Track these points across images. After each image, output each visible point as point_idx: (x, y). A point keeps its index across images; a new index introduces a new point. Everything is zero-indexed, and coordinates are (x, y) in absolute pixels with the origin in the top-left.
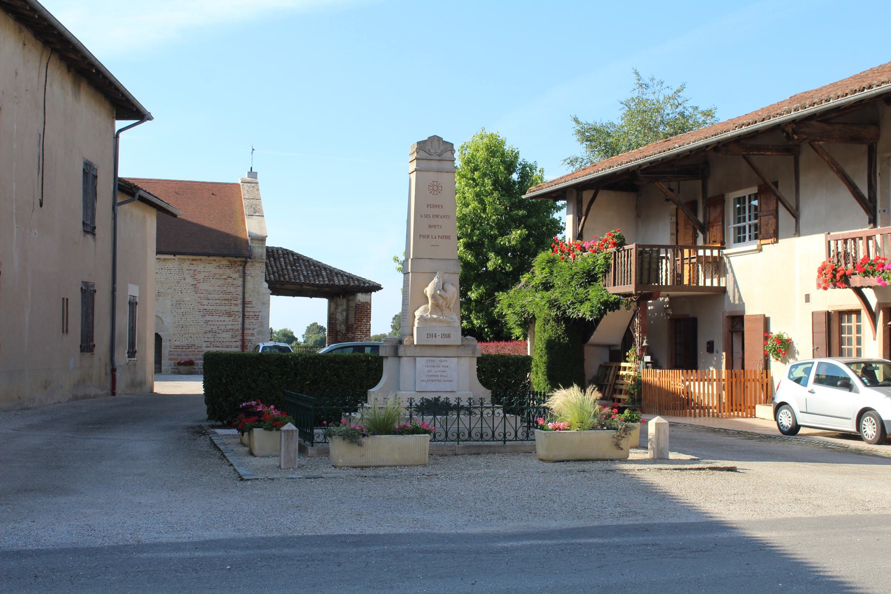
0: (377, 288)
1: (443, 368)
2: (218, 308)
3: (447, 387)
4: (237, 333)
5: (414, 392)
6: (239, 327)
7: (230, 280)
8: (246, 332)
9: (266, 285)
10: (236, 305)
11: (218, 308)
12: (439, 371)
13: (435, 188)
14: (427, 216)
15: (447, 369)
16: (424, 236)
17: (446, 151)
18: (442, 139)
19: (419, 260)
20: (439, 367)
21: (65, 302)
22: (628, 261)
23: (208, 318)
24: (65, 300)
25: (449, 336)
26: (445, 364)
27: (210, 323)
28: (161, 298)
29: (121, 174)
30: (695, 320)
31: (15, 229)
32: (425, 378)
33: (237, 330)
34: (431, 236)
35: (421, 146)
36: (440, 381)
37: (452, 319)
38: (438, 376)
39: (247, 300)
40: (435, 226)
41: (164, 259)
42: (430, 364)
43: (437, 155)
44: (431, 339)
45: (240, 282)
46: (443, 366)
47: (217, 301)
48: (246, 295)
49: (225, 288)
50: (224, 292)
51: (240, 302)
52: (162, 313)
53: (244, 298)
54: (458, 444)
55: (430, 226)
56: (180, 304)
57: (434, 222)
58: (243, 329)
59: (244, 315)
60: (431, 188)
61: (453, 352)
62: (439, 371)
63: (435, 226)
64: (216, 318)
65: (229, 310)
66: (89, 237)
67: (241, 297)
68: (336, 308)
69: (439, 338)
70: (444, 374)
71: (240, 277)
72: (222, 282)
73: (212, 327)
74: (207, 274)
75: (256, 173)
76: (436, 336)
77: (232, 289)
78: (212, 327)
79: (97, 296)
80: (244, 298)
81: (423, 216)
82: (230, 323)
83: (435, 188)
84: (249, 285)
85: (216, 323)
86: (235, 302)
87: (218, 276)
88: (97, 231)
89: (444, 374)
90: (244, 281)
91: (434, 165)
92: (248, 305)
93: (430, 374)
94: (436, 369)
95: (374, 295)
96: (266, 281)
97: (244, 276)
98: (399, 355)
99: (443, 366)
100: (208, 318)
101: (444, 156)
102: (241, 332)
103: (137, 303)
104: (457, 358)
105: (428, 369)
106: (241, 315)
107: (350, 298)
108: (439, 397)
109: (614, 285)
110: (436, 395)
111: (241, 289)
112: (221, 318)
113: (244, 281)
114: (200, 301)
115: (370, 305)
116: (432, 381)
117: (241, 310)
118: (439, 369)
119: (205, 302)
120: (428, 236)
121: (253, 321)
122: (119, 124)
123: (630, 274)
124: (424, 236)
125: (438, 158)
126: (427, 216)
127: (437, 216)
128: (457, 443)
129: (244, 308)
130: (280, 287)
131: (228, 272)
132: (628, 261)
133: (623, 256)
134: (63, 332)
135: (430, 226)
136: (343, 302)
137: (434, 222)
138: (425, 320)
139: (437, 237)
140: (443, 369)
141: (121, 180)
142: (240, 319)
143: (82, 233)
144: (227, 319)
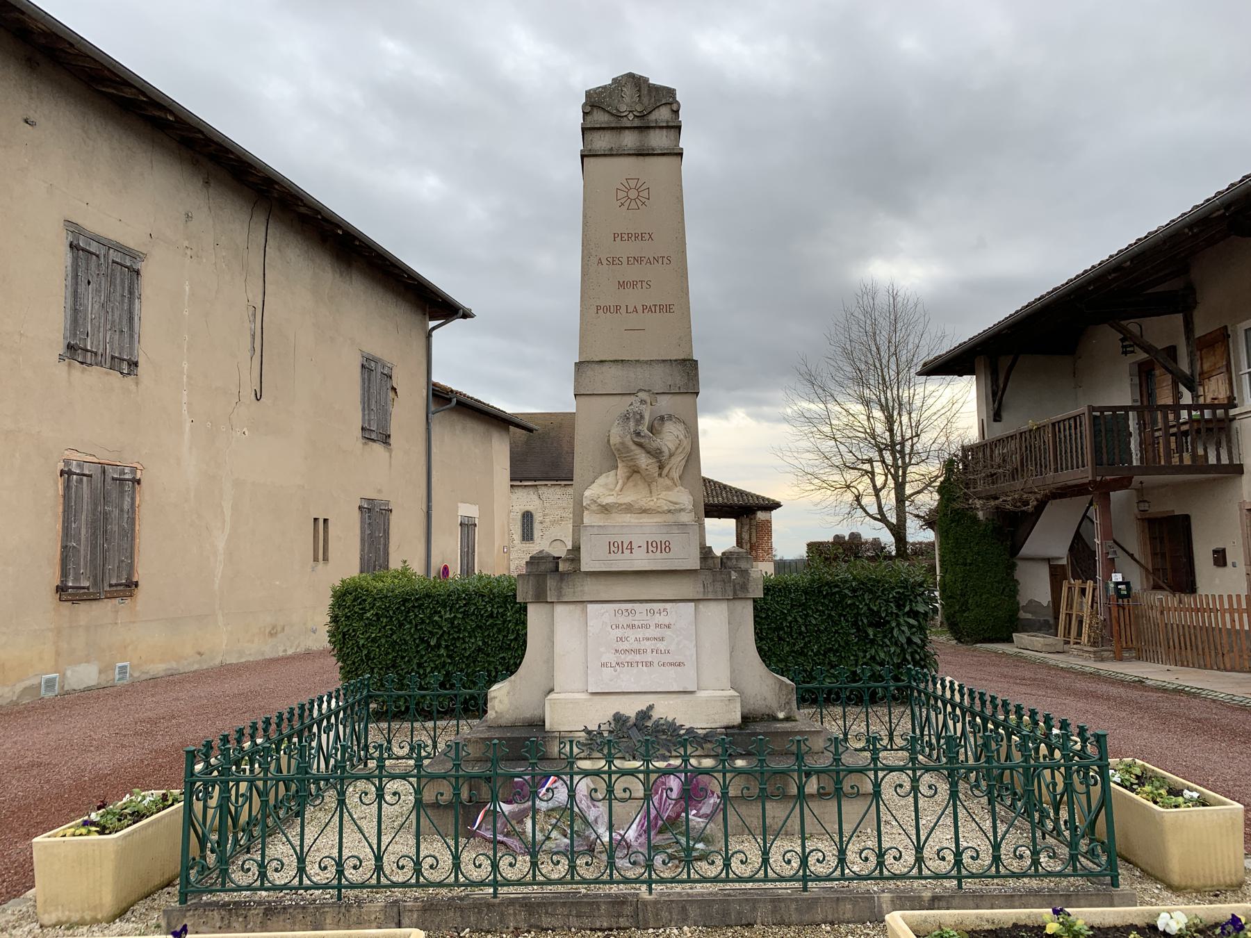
0: (777, 505)
3: (670, 679)
5: (584, 696)
12: (648, 639)
13: (633, 194)
14: (613, 261)
15: (668, 632)
16: (607, 309)
18: (646, 80)
19: (596, 366)
20: (647, 627)
21: (321, 526)
22: (1076, 434)
24: (321, 522)
25: (665, 547)
29: (435, 379)
30: (1186, 519)
31: (188, 425)
32: (610, 657)
34: (623, 310)
35: (595, 102)
36: (651, 663)
38: (645, 651)
40: (634, 284)
42: (622, 620)
43: (635, 116)
44: (619, 555)
46: (657, 626)
55: (622, 285)
61: (687, 588)
62: (648, 639)
63: (634, 284)
66: (378, 448)
68: (742, 528)
70: (661, 646)
76: (631, 549)
79: (394, 518)
81: (605, 262)
83: (633, 194)
88: (392, 441)
89: (661, 646)
91: (629, 140)
93: (626, 646)
94: (640, 634)
95: (774, 512)
98: (549, 600)
99: (657, 626)
101: (653, 117)
103: (475, 525)
104: (693, 604)
105: (619, 633)
107: (752, 517)
108: (651, 707)
109: (1056, 470)
110: (638, 705)
115: (770, 522)
116: (631, 664)
120: (618, 309)
122: (432, 324)
123: (1082, 453)
124: (607, 309)
125: (637, 123)
126: (613, 261)
127: (639, 260)
128: (644, 887)
132: (1076, 434)
133: (1067, 427)
134: (316, 559)
135: (622, 285)
136: (745, 520)
138: (603, 506)
139: (640, 309)
140: (657, 633)
141: (435, 385)
143: (361, 441)
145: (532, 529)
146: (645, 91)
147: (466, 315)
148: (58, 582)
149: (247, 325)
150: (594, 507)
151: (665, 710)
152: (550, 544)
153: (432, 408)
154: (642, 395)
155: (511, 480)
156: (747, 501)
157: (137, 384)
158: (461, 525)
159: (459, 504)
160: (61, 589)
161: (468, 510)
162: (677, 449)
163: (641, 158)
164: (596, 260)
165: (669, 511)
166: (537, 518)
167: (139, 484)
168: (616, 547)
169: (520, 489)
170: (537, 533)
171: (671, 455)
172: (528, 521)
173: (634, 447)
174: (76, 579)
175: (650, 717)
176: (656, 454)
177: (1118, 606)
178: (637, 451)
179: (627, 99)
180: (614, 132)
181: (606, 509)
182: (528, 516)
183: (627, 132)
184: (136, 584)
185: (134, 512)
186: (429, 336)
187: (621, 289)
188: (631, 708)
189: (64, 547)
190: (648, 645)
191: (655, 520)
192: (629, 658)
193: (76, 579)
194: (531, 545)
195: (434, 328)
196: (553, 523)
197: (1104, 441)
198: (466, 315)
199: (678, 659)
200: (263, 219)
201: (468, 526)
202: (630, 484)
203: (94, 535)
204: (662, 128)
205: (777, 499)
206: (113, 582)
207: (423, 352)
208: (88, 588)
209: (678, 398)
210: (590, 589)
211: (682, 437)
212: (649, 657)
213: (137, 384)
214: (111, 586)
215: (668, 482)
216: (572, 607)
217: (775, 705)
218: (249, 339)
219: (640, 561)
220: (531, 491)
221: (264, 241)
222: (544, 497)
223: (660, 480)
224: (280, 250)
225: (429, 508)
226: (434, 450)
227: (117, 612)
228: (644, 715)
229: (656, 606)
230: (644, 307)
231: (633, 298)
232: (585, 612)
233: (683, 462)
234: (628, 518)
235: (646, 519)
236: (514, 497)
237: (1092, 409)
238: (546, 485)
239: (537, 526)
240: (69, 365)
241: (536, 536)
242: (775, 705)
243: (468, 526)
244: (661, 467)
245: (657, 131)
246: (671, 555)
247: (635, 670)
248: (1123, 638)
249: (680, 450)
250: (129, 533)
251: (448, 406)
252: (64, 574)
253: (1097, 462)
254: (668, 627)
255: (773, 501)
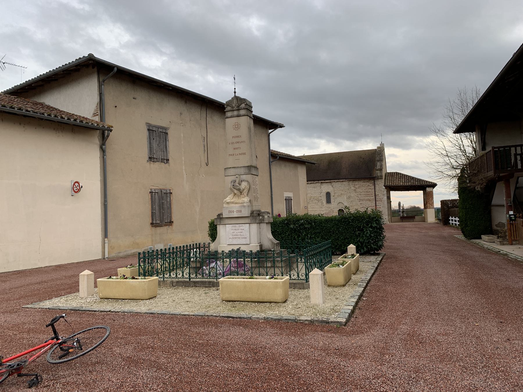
1: (241, 230)
2: (365, 198)
3: (244, 241)
4: (374, 207)
5: (226, 245)
6: (374, 205)
7: (369, 187)
8: (377, 207)
9: (384, 188)
10: (372, 196)
11: (365, 198)
12: (239, 232)
13: (237, 126)
14: (233, 143)
16: (231, 155)
17: (242, 104)
19: (229, 169)
20: (239, 230)
23: (361, 202)
25: (241, 211)
26: (243, 228)
27: (362, 204)
28: (342, 196)
31: (185, 176)
32: (231, 237)
33: (374, 206)
37: (244, 201)
39: (376, 194)
40: (237, 148)
41: (342, 181)
42: (234, 228)
45: (373, 187)
46: (241, 229)
47: (364, 196)
48: (376, 192)
49: (367, 190)
50: (367, 192)
51: (374, 195)
52: (343, 201)
53: (375, 193)
54: (217, 280)
55: (234, 149)
56: (350, 198)
57: (237, 146)
58: (376, 206)
59: (376, 200)
60: (234, 127)
61: (247, 221)
62: (239, 232)
63: (237, 148)
64: (365, 202)
65: (369, 198)
67: (374, 193)
69: (235, 213)
70: (242, 234)
71: (373, 185)
72: (366, 188)
73: (363, 206)
74: (360, 185)
75: (384, 144)
77: (370, 190)
78: (363, 206)
80: (375, 193)
82: (370, 204)
83: (237, 126)
84: (377, 188)
85: (365, 204)
86: (372, 195)
87: (364, 186)
89: (242, 234)
90: (375, 187)
91: (235, 113)
92: (377, 196)
93: (234, 234)
96: (384, 186)
97: (374, 185)
99: (241, 229)
100: (361, 202)
101: (241, 106)
102: (375, 207)
104: (248, 224)
105: (233, 231)
106: (374, 200)
108: (240, 248)
109: (487, 172)
110: (237, 247)
111: (373, 190)
112: (367, 202)
113: (375, 187)
114: (358, 196)
116: (235, 238)
117: (374, 198)
118: (239, 231)
119: (360, 196)
121: (380, 202)
122: (270, 131)
124: (231, 155)
126: (233, 143)
127: (238, 142)
129: (375, 197)
130: (390, 188)
131: (368, 184)
135: (234, 149)
137: (237, 146)
139: (238, 154)
140: (241, 231)
142: (374, 202)
144: (369, 202)
145: (330, 199)
146: (239, 100)
147: (285, 126)
148: (151, 222)
149: (202, 143)
150: (225, 203)
151: (243, 248)
152: (338, 204)
153: (271, 160)
154: (237, 176)
155: (307, 181)
156: (421, 183)
157: (169, 166)
158: (285, 199)
159: (284, 193)
160: (152, 224)
161: (290, 195)
162: (245, 188)
163: (238, 117)
164: (228, 143)
165: (242, 203)
166: (332, 194)
167: (172, 194)
168: (230, 212)
169: (325, 184)
170: (332, 200)
171: (244, 190)
172: (328, 196)
173: (233, 189)
174: (156, 221)
175: (239, 250)
176: (239, 190)
177: (510, 224)
178: (234, 189)
179: (235, 103)
180: (232, 111)
181: (228, 203)
182: (328, 194)
183: (235, 111)
184: (173, 222)
185: (171, 202)
186: (269, 136)
187: (234, 150)
188: (235, 248)
189: (152, 212)
190: (239, 234)
191: (239, 205)
192: (235, 237)
193: (156, 221)
194: (330, 205)
195: (270, 133)
196: (338, 196)
197: (500, 160)
198: (284, 127)
199: (245, 237)
200: (205, 109)
201: (288, 200)
202: (235, 197)
203: (160, 209)
204: (242, 109)
205: (435, 182)
206: (166, 221)
207: (267, 142)
208: (159, 223)
209: (247, 175)
210: (227, 221)
211: (246, 185)
212: (239, 237)
213: (169, 166)
214: (165, 222)
215: (243, 196)
216: (223, 225)
217: (271, 248)
218: (203, 148)
219: (235, 215)
220: (329, 184)
221: (206, 116)
222: (334, 186)
223: (241, 196)
224: (211, 118)
225: (272, 195)
226: (273, 175)
227: (168, 229)
228: (238, 249)
229: (240, 225)
230: (239, 154)
231: (237, 152)
232: (226, 226)
233: (247, 191)
234: (233, 205)
235: (237, 205)
236: (322, 187)
237: (494, 148)
238: (335, 182)
239: (332, 198)
240: (150, 163)
241: (332, 201)
242: (271, 248)
243: (288, 200)
244: (241, 193)
245: (242, 110)
246: (241, 213)
247: (236, 239)
248: (513, 236)
249: (246, 188)
250: (170, 208)
251: (276, 159)
252: (153, 220)
253: (496, 168)
254: (243, 229)
255: (433, 183)
